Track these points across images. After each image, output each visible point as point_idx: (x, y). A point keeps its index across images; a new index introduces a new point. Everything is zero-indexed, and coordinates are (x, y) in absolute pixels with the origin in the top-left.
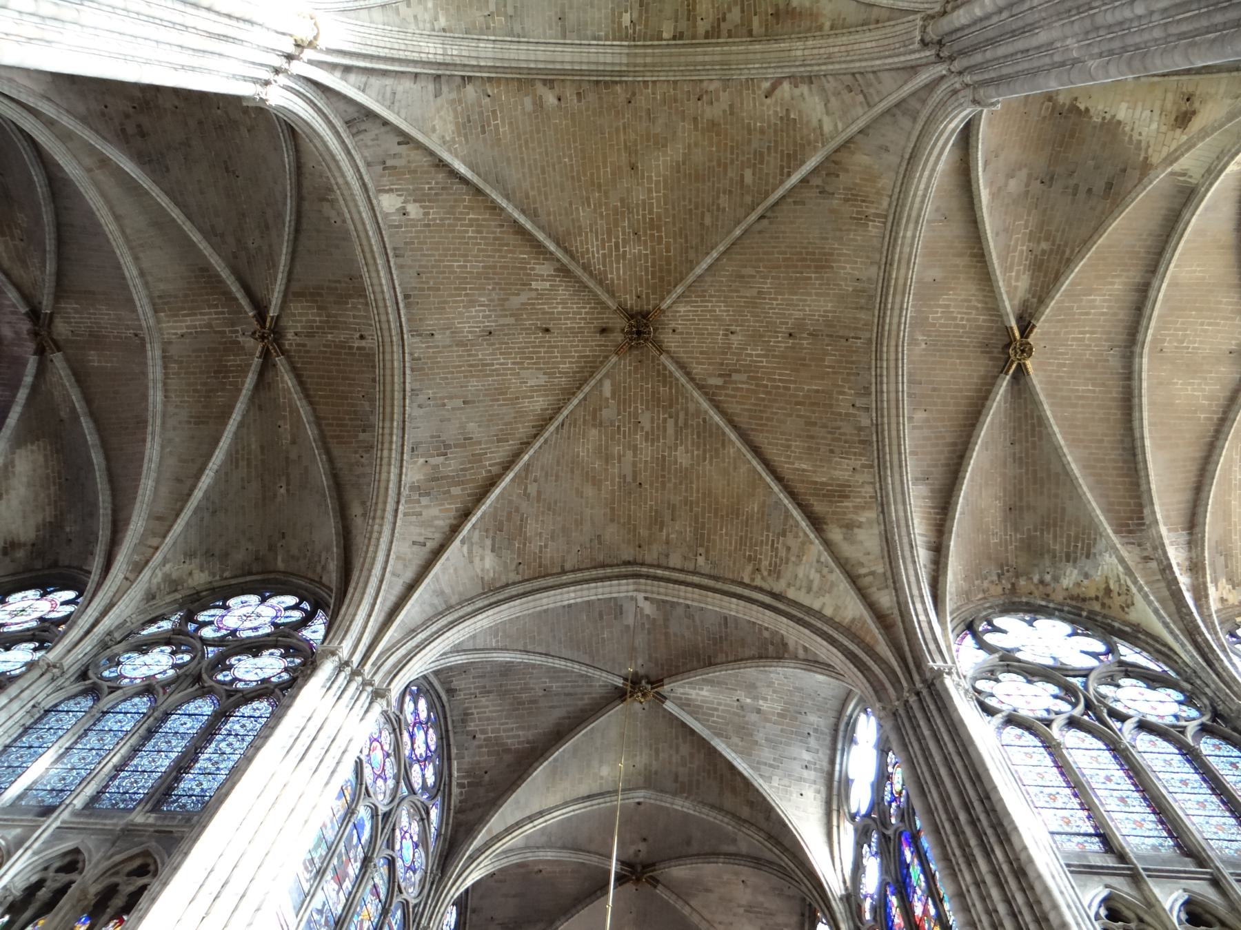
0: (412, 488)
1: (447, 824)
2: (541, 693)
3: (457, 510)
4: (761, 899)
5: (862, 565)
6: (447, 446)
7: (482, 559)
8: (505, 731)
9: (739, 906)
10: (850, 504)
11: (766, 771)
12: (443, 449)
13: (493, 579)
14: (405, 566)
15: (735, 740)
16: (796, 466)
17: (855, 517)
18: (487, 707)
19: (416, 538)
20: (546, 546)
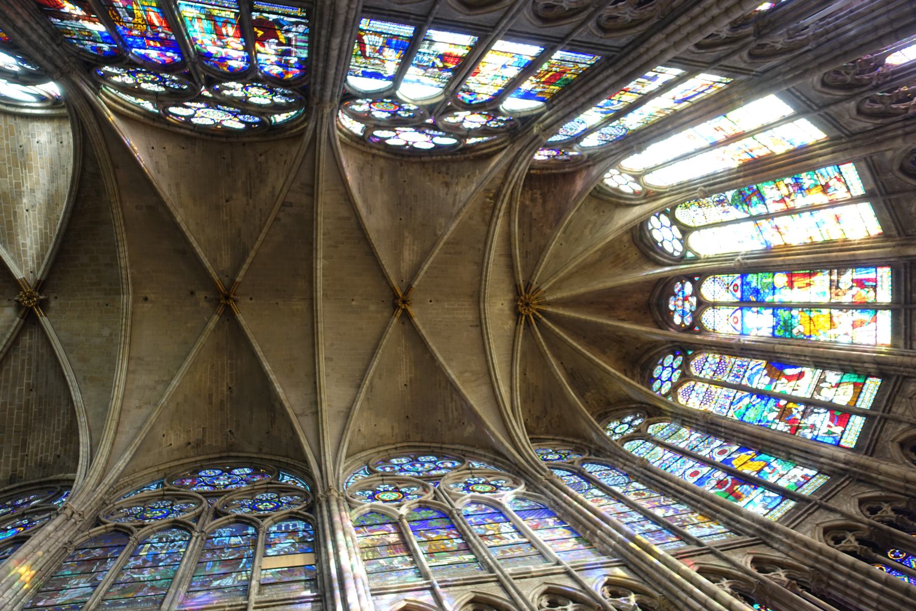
2: (34, 393)
4: (239, 184)
8: (58, 428)
9: (248, 204)
18: (38, 444)
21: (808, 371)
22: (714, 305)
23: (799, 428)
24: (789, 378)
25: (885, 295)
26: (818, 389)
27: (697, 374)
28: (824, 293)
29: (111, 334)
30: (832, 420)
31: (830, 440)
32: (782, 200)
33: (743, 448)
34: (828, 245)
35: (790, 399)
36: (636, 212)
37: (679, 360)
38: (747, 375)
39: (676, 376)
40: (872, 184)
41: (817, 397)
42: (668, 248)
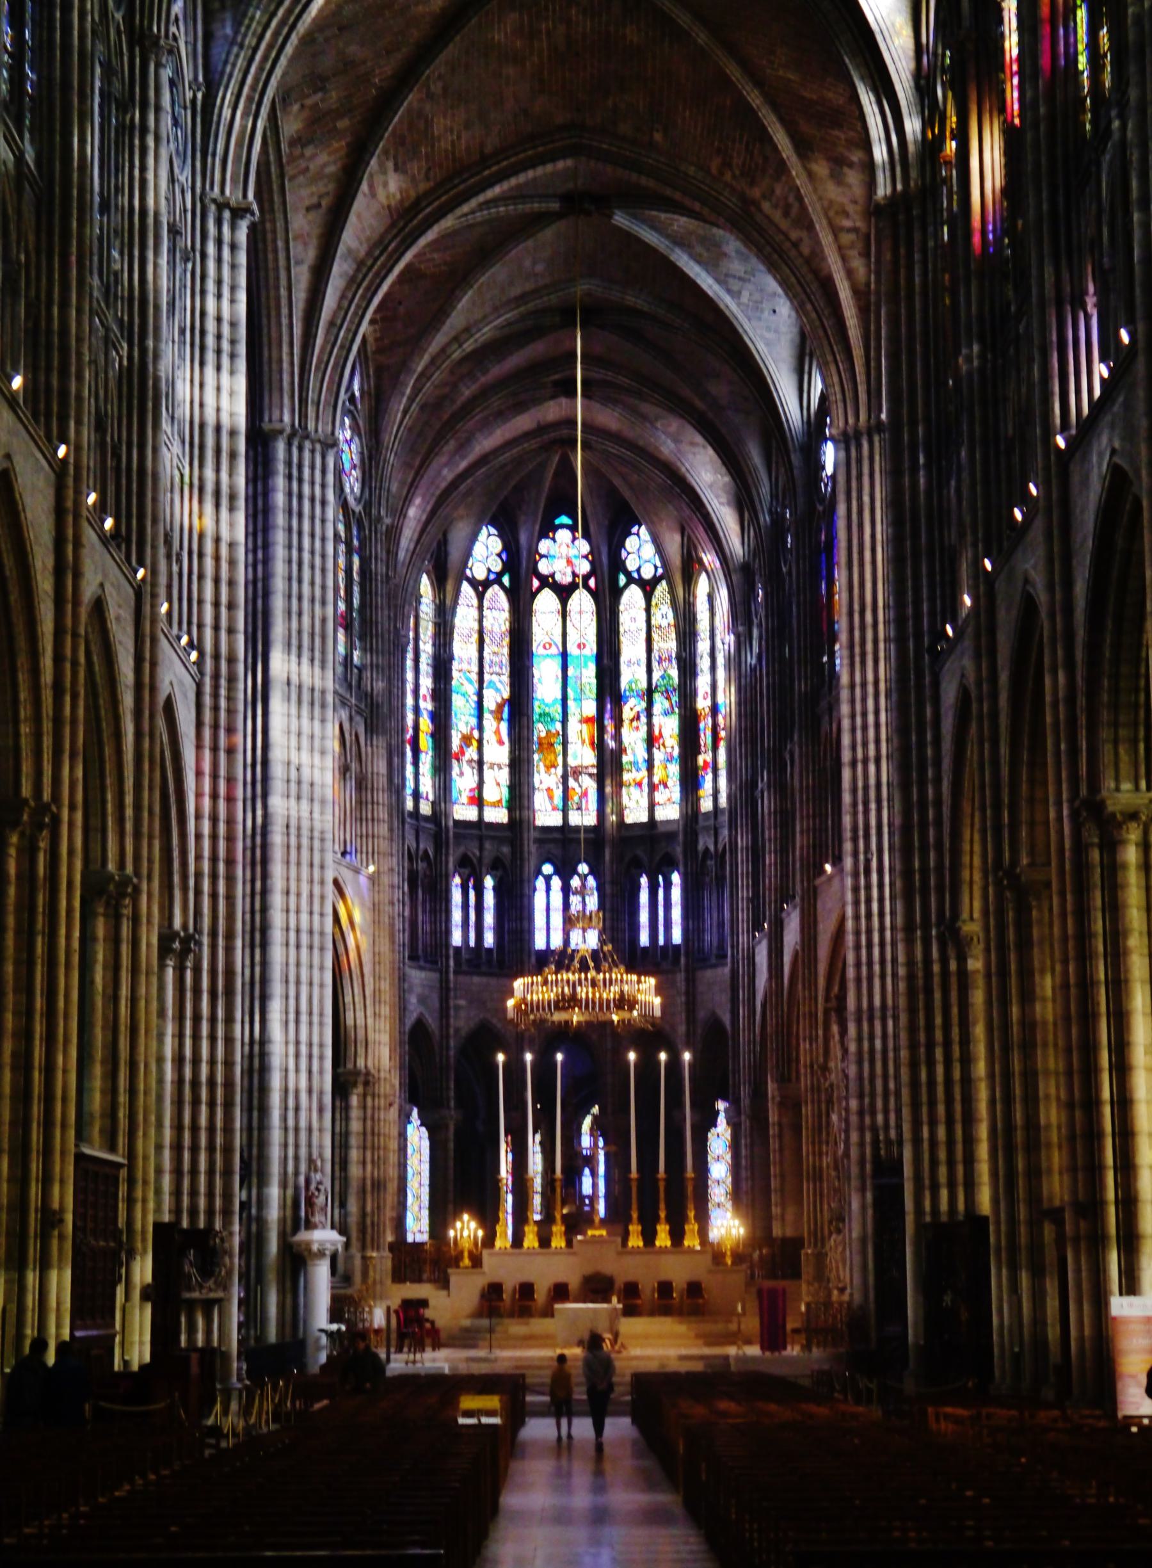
0: (292, 143)
1: (368, 376)
3: (348, 145)
5: (846, 215)
6: (324, 79)
7: (385, 185)
10: (843, 136)
11: (735, 285)
12: (317, 82)
13: (402, 201)
14: (305, 244)
15: (699, 249)
16: (781, 73)
17: (846, 153)
19: (307, 203)
20: (459, 138)
21: (506, 748)
22: (564, 614)
23: (458, 760)
24: (497, 732)
25: (575, 819)
26: (492, 766)
27: (486, 604)
28: (576, 757)
29: (536, 275)
30: (472, 790)
31: (454, 794)
32: (661, 735)
33: (434, 716)
34: (618, 768)
35: (480, 742)
36: (673, 543)
37: (497, 566)
38: (495, 678)
39: (480, 574)
40: (661, 829)
41: (485, 767)
42: (631, 543)
